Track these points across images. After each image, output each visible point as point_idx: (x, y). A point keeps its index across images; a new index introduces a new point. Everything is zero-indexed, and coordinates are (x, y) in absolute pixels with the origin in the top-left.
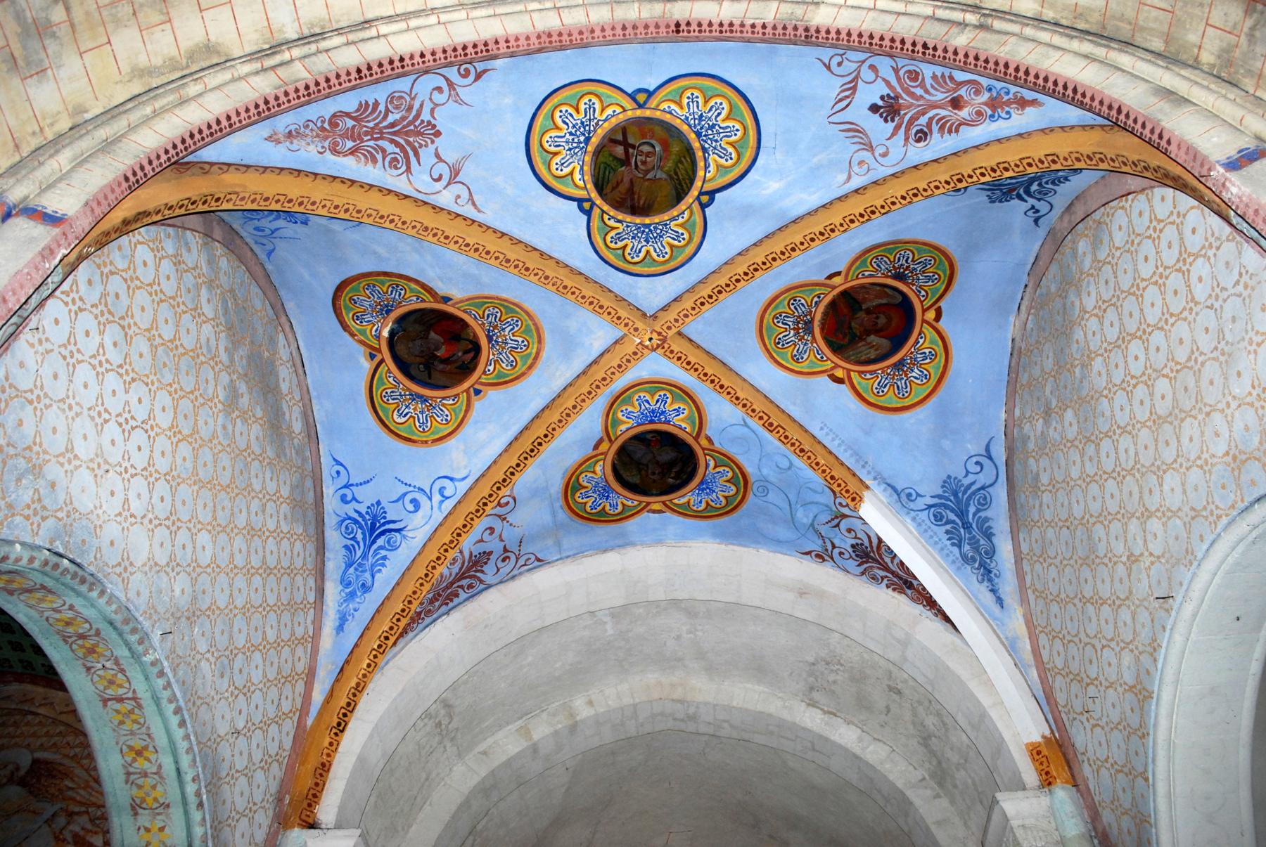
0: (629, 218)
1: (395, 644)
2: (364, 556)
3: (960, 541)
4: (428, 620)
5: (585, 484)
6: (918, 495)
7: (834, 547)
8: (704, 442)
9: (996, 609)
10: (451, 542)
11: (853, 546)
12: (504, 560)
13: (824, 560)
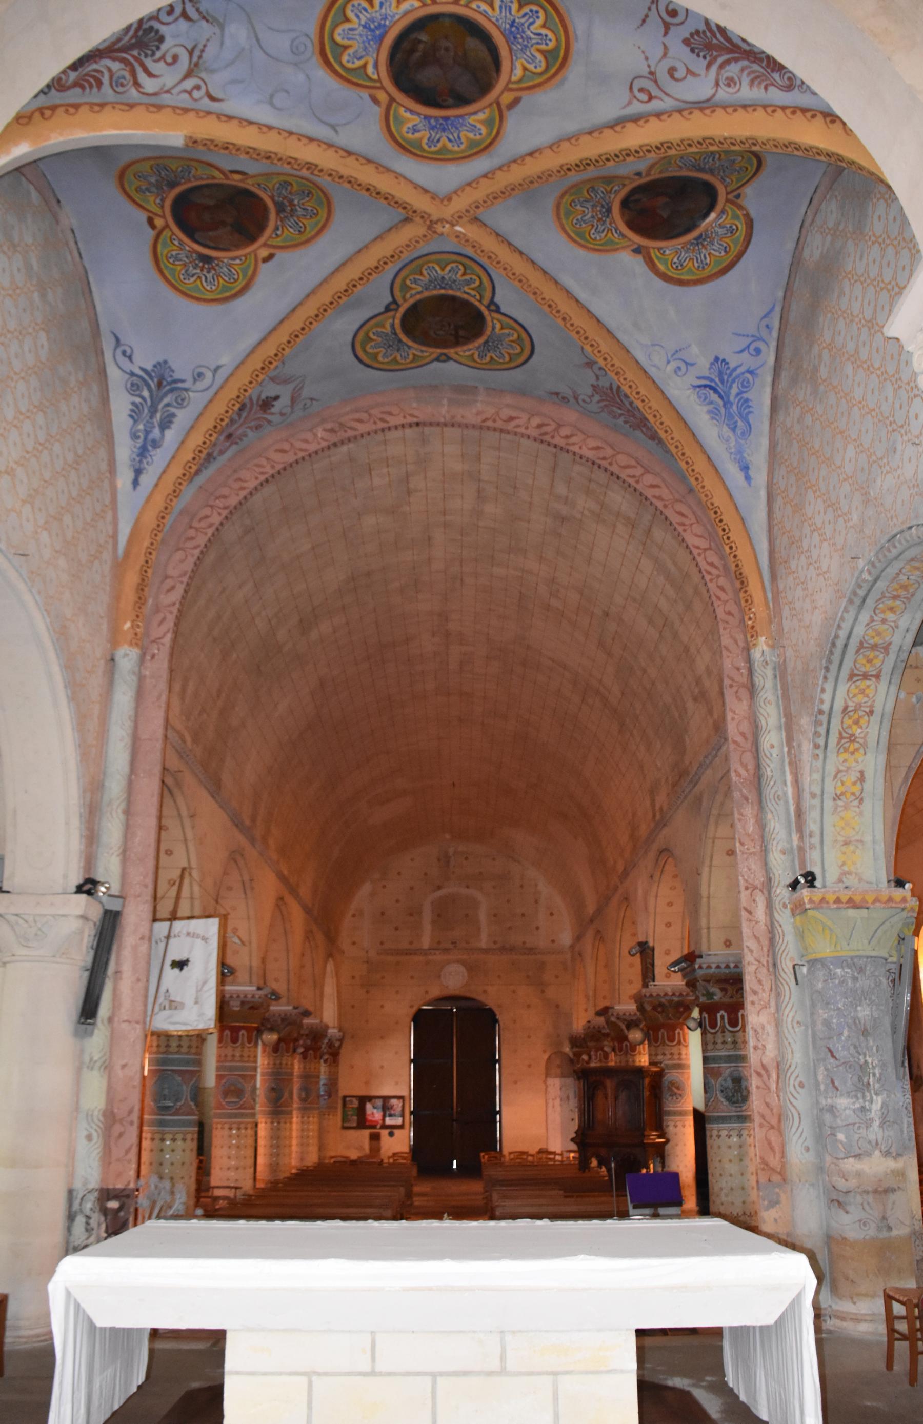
0: (458, 294)
5: (539, 57)
8: (382, 96)
11: (161, 39)
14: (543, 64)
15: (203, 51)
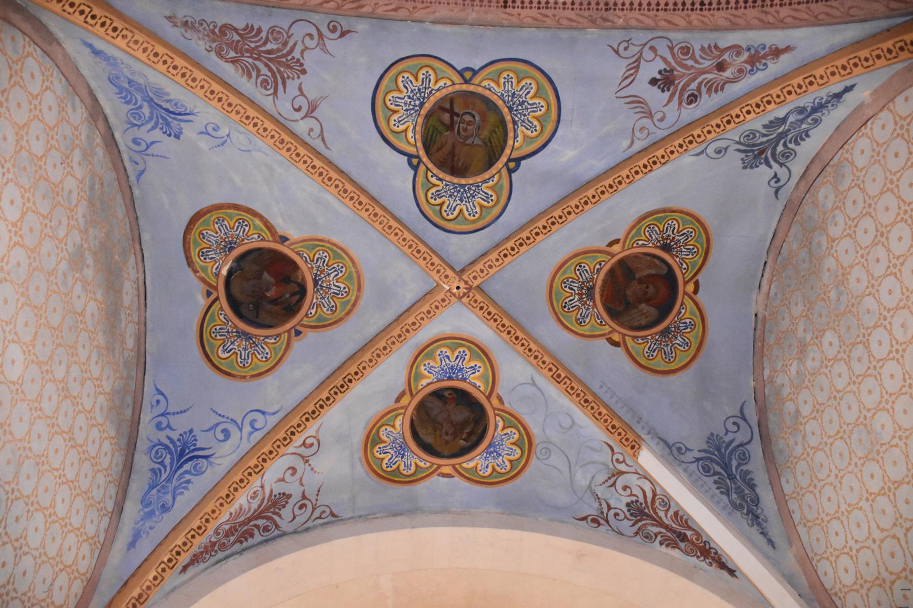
0: (448, 178)
1: (185, 568)
2: (169, 479)
3: (728, 490)
4: (221, 555)
5: (384, 438)
6: (687, 449)
7: (609, 508)
8: (495, 402)
9: (768, 548)
10: (256, 466)
11: (628, 505)
12: (301, 508)
13: (599, 524)
14: (381, 433)
15: (607, 481)
